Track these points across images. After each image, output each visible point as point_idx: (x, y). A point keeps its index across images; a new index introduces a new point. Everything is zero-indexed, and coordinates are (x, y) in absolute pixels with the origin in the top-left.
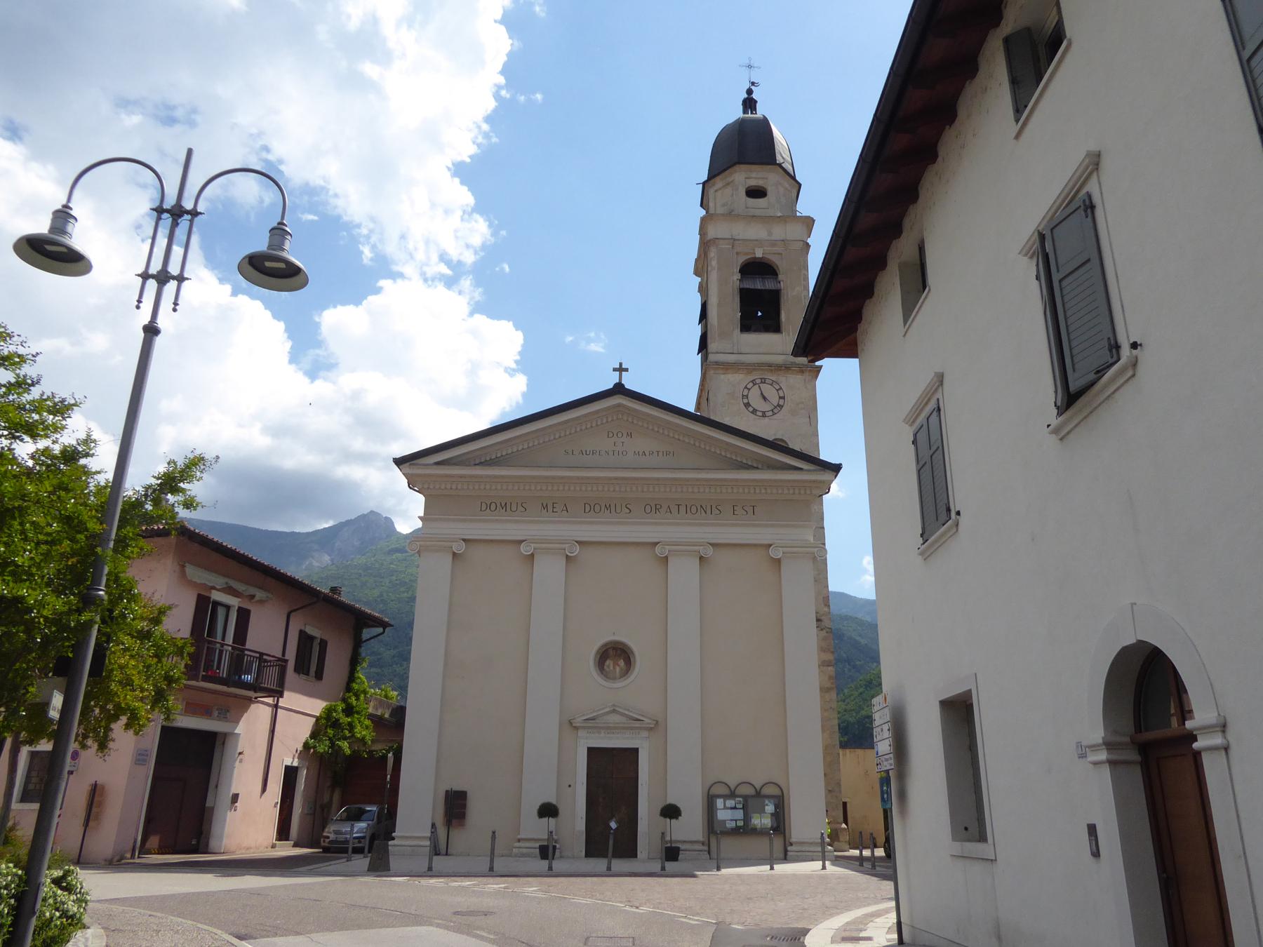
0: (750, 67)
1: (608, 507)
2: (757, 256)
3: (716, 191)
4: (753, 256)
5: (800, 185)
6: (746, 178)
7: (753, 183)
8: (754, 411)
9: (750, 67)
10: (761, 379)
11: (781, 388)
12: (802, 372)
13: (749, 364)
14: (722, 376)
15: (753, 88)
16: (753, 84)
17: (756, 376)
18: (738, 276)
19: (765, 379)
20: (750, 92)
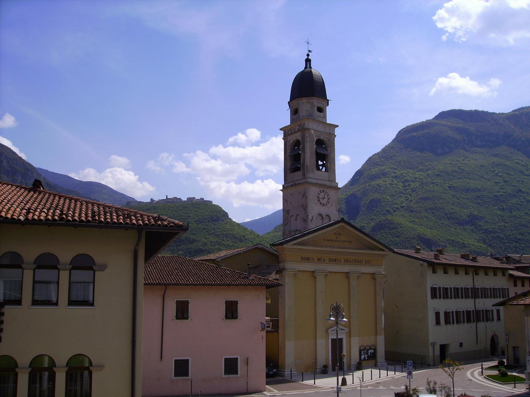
0: (308, 43)
1: (335, 260)
2: (321, 138)
3: (303, 103)
4: (319, 138)
5: (328, 105)
6: (317, 103)
7: (319, 105)
8: (321, 203)
9: (308, 43)
10: (323, 190)
11: (328, 195)
12: (335, 189)
13: (321, 185)
14: (311, 188)
15: (309, 53)
16: (309, 51)
17: (321, 189)
18: (315, 146)
19: (324, 191)
20: (308, 55)
